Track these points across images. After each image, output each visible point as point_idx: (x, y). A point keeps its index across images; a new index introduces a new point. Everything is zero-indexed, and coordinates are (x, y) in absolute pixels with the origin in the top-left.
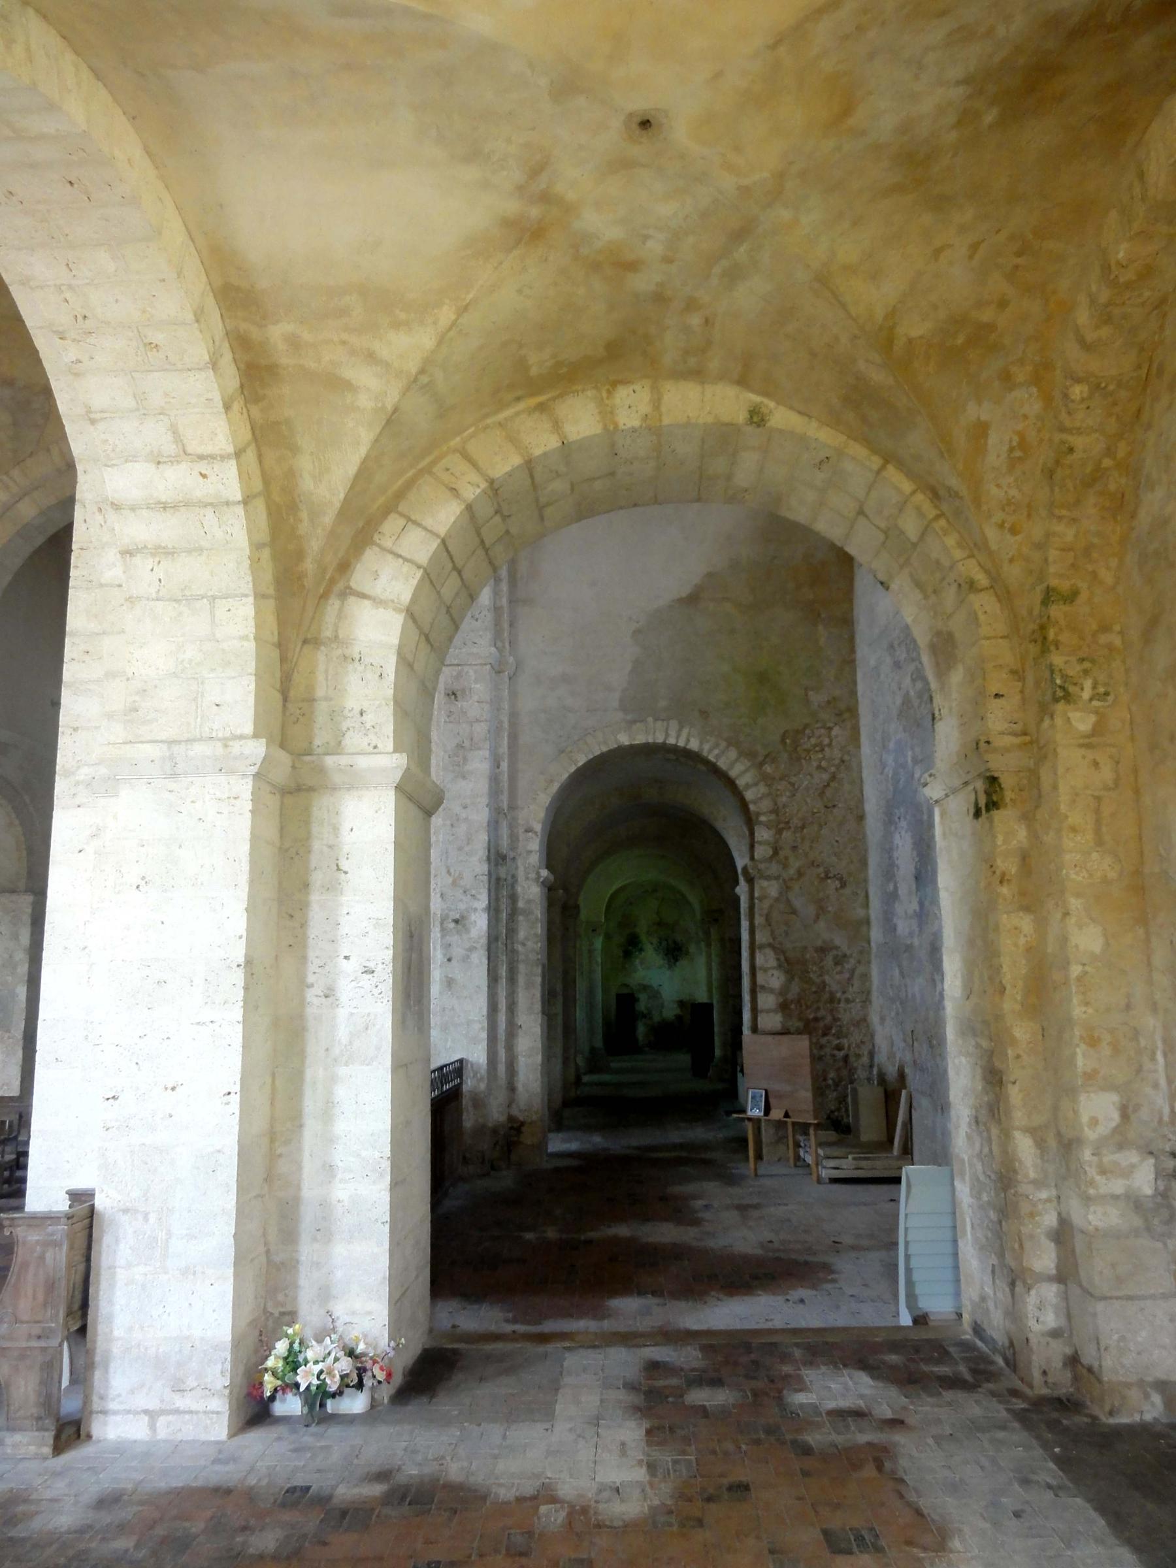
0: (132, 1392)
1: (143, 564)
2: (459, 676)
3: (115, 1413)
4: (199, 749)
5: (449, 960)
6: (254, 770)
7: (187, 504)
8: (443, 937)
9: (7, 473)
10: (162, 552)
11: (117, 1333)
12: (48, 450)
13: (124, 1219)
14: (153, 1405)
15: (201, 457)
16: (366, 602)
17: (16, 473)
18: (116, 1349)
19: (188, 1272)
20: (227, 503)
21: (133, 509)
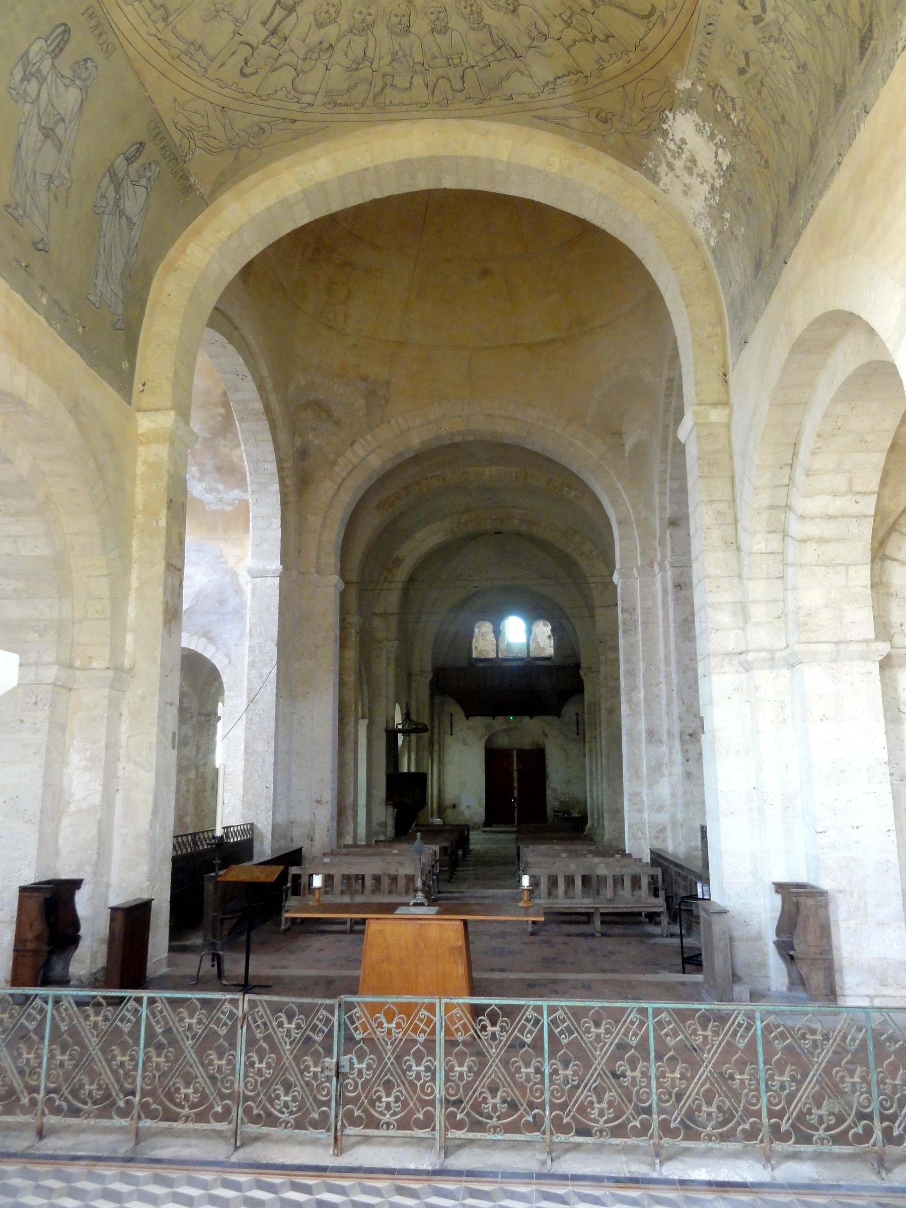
0: (858, 985)
1: (810, 547)
2: (682, 574)
3: (850, 996)
4: (853, 647)
5: (688, 760)
6: (881, 658)
7: (843, 516)
8: (682, 745)
9: (363, 438)
10: (822, 540)
11: (844, 955)
12: (389, 422)
13: (840, 896)
14: (871, 992)
15: (859, 493)
16: (896, 563)
17: (368, 437)
18: (845, 963)
19: (880, 924)
20: (865, 516)
21: (812, 518)
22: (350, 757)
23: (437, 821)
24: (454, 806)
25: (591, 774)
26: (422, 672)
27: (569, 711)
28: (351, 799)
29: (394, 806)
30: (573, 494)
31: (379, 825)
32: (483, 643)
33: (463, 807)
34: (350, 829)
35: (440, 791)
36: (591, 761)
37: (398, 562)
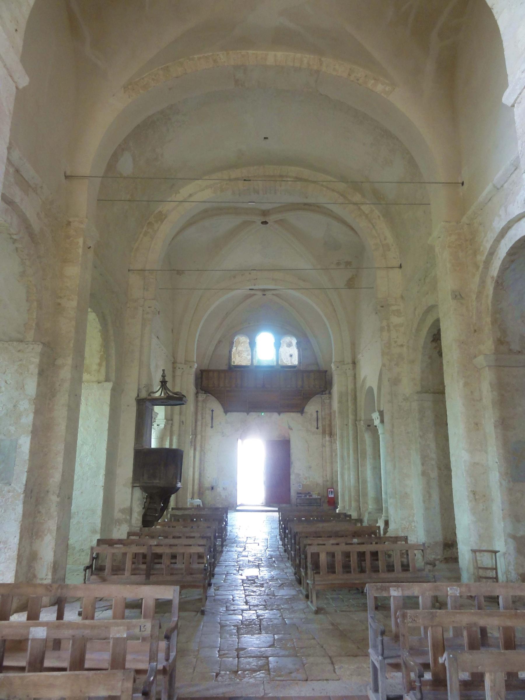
22: (60, 414)
23: (198, 501)
24: (212, 488)
25: (342, 458)
26: (186, 362)
27: (311, 408)
28: (56, 477)
29: (144, 489)
30: (379, 88)
31: (122, 511)
32: (241, 356)
33: (220, 490)
34: (52, 525)
35: (200, 474)
36: (342, 448)
37: (161, 217)
